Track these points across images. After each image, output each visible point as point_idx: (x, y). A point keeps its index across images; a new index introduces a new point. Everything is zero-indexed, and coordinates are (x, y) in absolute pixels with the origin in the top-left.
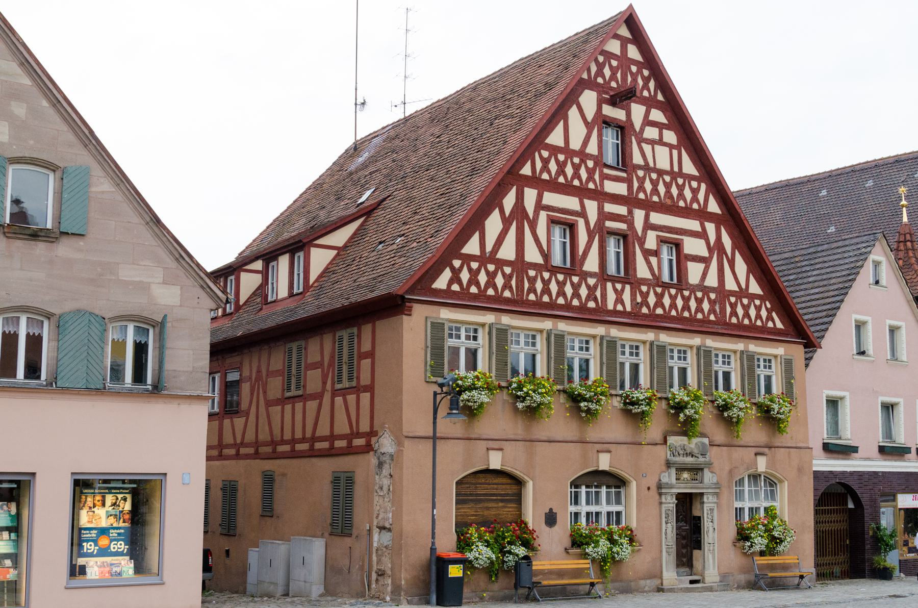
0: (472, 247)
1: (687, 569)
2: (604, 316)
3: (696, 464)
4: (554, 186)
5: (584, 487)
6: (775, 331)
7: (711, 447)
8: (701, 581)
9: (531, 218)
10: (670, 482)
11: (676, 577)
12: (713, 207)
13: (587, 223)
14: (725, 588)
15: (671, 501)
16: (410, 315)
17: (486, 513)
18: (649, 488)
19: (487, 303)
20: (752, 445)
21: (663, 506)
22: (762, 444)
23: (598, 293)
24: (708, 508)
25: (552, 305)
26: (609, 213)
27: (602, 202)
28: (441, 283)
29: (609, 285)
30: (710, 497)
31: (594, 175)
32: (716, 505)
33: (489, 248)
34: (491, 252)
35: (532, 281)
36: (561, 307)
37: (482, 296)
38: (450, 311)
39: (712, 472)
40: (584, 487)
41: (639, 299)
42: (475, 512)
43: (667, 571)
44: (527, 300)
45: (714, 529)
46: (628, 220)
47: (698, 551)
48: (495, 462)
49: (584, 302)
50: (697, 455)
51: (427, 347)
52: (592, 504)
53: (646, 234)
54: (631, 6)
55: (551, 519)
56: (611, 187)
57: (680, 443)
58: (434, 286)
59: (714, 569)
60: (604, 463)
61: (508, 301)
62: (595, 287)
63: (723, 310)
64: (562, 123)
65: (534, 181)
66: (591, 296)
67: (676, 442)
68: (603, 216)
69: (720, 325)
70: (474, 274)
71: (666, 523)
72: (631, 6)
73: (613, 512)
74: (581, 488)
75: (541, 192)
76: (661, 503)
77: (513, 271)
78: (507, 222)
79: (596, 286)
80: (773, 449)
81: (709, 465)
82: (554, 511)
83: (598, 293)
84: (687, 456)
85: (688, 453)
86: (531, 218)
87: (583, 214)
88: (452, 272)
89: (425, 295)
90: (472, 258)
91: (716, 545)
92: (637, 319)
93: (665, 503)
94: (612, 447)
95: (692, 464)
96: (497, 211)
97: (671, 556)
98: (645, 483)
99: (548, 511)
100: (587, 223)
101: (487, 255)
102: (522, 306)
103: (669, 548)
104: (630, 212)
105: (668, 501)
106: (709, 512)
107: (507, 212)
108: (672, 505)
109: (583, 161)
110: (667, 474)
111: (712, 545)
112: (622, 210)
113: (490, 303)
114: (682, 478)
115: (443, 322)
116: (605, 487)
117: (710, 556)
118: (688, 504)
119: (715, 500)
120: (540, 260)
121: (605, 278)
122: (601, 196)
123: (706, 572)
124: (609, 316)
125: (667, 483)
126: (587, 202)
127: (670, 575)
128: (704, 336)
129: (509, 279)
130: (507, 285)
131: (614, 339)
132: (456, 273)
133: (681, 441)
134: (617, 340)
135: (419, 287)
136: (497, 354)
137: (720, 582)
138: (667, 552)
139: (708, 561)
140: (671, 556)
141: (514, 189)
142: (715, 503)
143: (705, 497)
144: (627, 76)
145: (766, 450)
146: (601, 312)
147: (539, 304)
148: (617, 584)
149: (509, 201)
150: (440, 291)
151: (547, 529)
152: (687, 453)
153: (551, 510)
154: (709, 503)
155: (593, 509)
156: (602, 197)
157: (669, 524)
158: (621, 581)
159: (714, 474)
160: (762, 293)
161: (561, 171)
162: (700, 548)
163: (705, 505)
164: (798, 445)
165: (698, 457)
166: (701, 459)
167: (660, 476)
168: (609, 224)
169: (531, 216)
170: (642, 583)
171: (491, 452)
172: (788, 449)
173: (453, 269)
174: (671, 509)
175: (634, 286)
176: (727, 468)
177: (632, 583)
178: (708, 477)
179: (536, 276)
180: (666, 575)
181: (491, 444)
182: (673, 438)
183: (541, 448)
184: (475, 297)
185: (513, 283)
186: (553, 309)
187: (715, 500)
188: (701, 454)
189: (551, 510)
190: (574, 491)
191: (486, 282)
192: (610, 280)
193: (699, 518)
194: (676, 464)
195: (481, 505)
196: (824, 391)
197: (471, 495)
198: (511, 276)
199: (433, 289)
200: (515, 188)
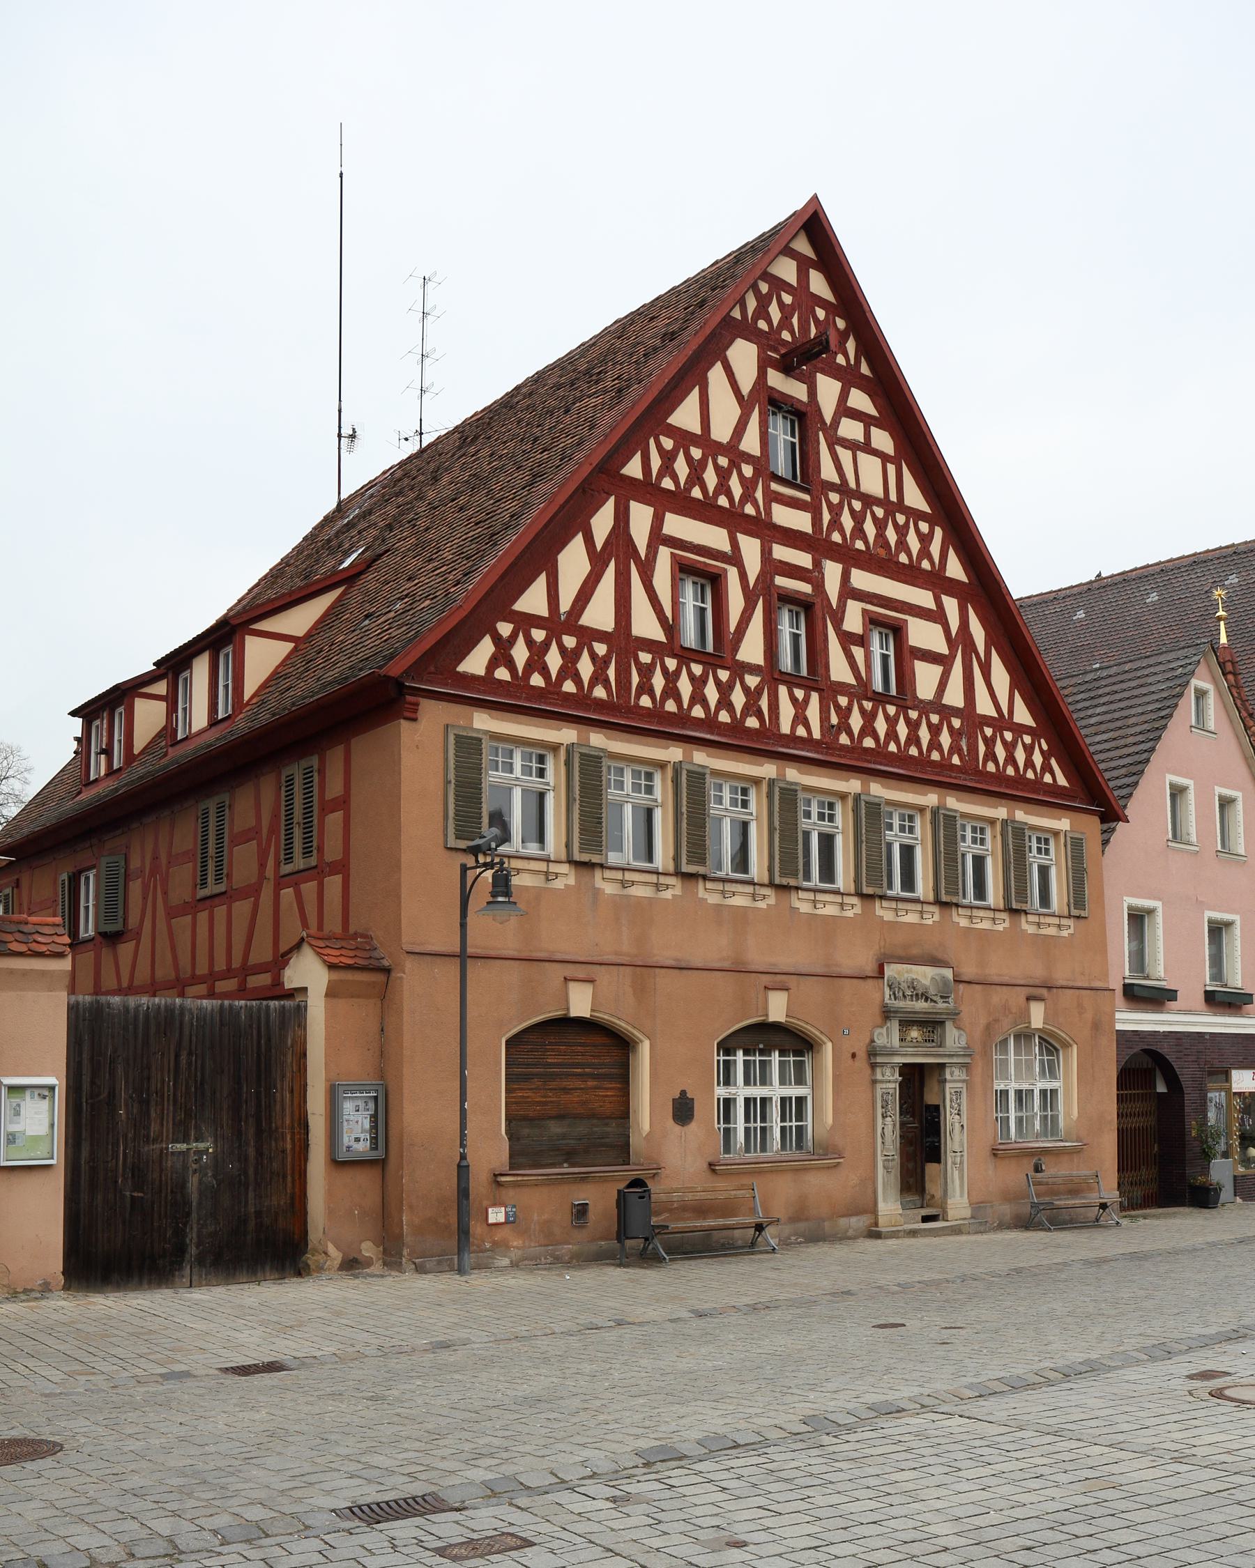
0: (533, 600)
1: (916, 1198)
4: (681, 503)
5: (740, 1053)
6: (1054, 789)
7: (957, 984)
8: (941, 1217)
10: (889, 1045)
11: (901, 1212)
12: (955, 569)
13: (743, 576)
14: (982, 1229)
15: (891, 1078)
16: (415, 720)
18: (854, 1056)
19: (562, 706)
20: (1022, 982)
21: (879, 1086)
22: (1037, 982)
23: (764, 704)
24: (953, 1091)
25: (683, 718)
26: (780, 561)
27: (770, 541)
28: (476, 662)
29: (783, 690)
30: (957, 1072)
31: (754, 491)
33: (565, 605)
34: (569, 613)
35: (646, 671)
36: (698, 723)
37: (553, 693)
38: (492, 717)
39: (958, 1028)
40: (740, 1053)
41: (834, 720)
42: (542, 1097)
43: (885, 1200)
44: (637, 706)
45: (962, 1126)
46: (814, 576)
47: (935, 1165)
48: (580, 1004)
50: (934, 998)
51: (448, 782)
52: (755, 1084)
53: (845, 606)
54: (815, 199)
56: (784, 516)
57: (906, 975)
58: (462, 668)
59: (962, 1195)
60: (777, 1009)
61: (599, 703)
62: (759, 691)
63: (973, 749)
64: (696, 391)
65: (647, 490)
66: (752, 707)
67: (899, 973)
68: (771, 566)
69: (969, 774)
70: (538, 653)
71: (884, 1117)
72: (815, 199)
73: (791, 1098)
74: (735, 1055)
75: (660, 512)
76: (874, 1082)
77: (609, 652)
78: (598, 561)
79: (759, 691)
80: (1055, 990)
81: (954, 1015)
82: (689, 1096)
83: (764, 704)
84: (917, 1000)
85: (920, 993)
87: (735, 558)
91: (965, 1153)
93: (882, 1082)
94: (792, 981)
95: (925, 1013)
96: (579, 540)
99: (677, 1095)
100: (743, 576)
102: (627, 718)
103: (888, 1160)
104: (817, 564)
105: (886, 1078)
106: (954, 1098)
108: (893, 1085)
109: (735, 464)
111: (959, 1154)
112: (803, 559)
113: (569, 708)
114: (909, 1039)
115: (480, 736)
116: (777, 1053)
117: (956, 1173)
118: (917, 1084)
119: (964, 1077)
120: (658, 635)
121: (776, 677)
122: (769, 532)
123: (949, 1201)
124: (783, 746)
125: (885, 1047)
127: (889, 1207)
128: (944, 791)
129: (600, 664)
130: (599, 677)
131: (793, 787)
133: (907, 972)
134: (798, 788)
135: (432, 669)
136: (581, 801)
137: (972, 1217)
138: (884, 1167)
139: (953, 1182)
141: (611, 503)
142: (963, 1081)
143: (948, 1071)
144: (810, 325)
145: (1044, 992)
146: (769, 738)
147: (656, 713)
148: (802, 1226)
149: (602, 522)
150: (474, 678)
151: (677, 1128)
152: (917, 995)
153: (683, 1093)
155: (757, 1092)
156: (769, 533)
157: (889, 1119)
158: (807, 1220)
159: (962, 1032)
161: (696, 476)
162: (939, 1161)
163: (948, 1085)
165: (935, 1002)
166: (941, 1005)
167: (872, 1035)
168: (780, 581)
169: (642, 553)
170: (843, 1222)
171: (572, 985)
172: (1077, 991)
173: (497, 638)
174: (891, 1091)
176: (983, 1021)
177: (826, 1223)
178: (953, 1038)
179: (653, 664)
180: (882, 1206)
181: (570, 971)
182: (894, 966)
183: (665, 982)
185: (611, 673)
187: (964, 1077)
188: (942, 997)
189: (683, 1093)
190: (724, 1060)
191: (561, 667)
192: (785, 682)
193: (937, 1108)
194: (901, 1012)
195: (553, 1085)
196: (1125, 898)
197: (535, 1065)
199: (459, 672)
200: (612, 500)
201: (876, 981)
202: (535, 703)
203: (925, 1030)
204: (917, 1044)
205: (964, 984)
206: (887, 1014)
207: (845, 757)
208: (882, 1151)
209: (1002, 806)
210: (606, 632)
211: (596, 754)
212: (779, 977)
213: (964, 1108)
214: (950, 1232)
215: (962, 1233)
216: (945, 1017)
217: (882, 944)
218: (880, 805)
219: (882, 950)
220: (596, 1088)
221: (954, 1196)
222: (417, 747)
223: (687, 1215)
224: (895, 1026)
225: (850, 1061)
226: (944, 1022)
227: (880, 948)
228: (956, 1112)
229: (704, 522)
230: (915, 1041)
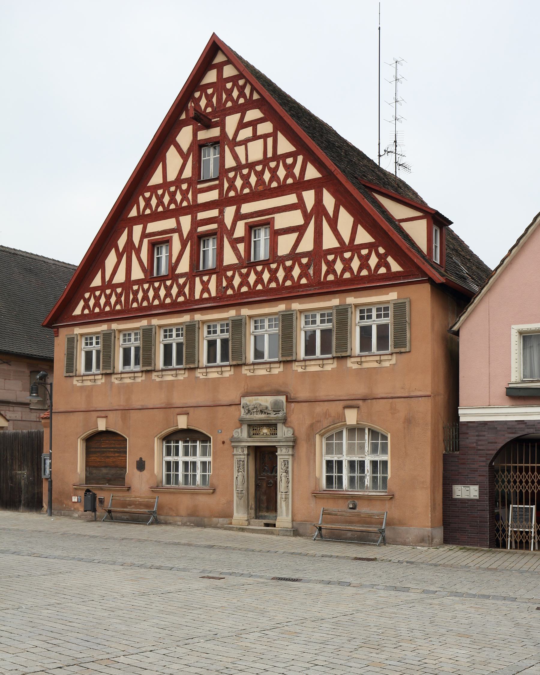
0: (97, 282)
2: (192, 306)
3: (268, 420)
4: (156, 217)
5: (198, 442)
6: (397, 275)
7: (290, 403)
9: (137, 247)
15: (241, 453)
16: (58, 336)
17: (107, 460)
18: (223, 443)
19: (105, 317)
20: (345, 398)
22: (359, 397)
23: (187, 290)
24: (282, 460)
25: (151, 307)
26: (201, 220)
28: (78, 311)
29: (197, 279)
30: (284, 450)
32: (291, 457)
33: (107, 278)
34: (108, 281)
35: (136, 293)
37: (102, 313)
38: (80, 329)
39: (287, 427)
41: (225, 284)
42: (100, 459)
43: (237, 512)
44: (131, 308)
48: (102, 426)
49: (174, 298)
52: (191, 456)
55: (141, 465)
56: (202, 198)
59: (287, 515)
60: (182, 423)
61: (119, 312)
63: (318, 271)
67: (250, 401)
68: (195, 224)
69: (314, 286)
70: (97, 299)
76: (234, 455)
78: (120, 257)
80: (369, 401)
81: (285, 421)
82: (143, 460)
83: (187, 290)
86: (137, 247)
87: (178, 230)
88: (84, 302)
89: (71, 321)
90: (96, 288)
92: (222, 302)
94: (191, 411)
95: (263, 420)
96: (113, 251)
97: (242, 500)
98: (220, 438)
99: (138, 459)
101: (106, 283)
103: (238, 493)
106: (283, 464)
107: (121, 249)
108: (243, 457)
109: (178, 187)
110: (239, 430)
112: (214, 213)
113: (108, 317)
114: (262, 433)
117: (284, 504)
124: (196, 305)
126: (182, 219)
129: (119, 296)
130: (118, 302)
132: (87, 301)
133: (255, 400)
135: (66, 317)
136: (103, 351)
138: (237, 496)
139: (281, 508)
140: (242, 500)
143: (279, 450)
145: (360, 403)
147: (140, 308)
148: (193, 519)
150: (78, 316)
151: (138, 472)
153: (141, 459)
154: (282, 455)
155: (190, 459)
156: (196, 209)
157: (240, 473)
158: (197, 516)
160: (373, 240)
161: (160, 202)
164: (412, 394)
166: (273, 415)
168: (200, 229)
169: (137, 246)
170: (215, 520)
171: (99, 419)
172: (391, 400)
174: (242, 460)
175: (220, 274)
176: (308, 422)
177: (206, 519)
178: (283, 432)
180: (235, 515)
181: (99, 414)
182: (247, 398)
183: (134, 415)
184: (98, 314)
185: (123, 299)
186: (151, 310)
189: (141, 459)
191: (105, 303)
195: (104, 455)
198: (121, 294)
201: (237, 407)
202: (97, 319)
203: (271, 429)
204: (266, 436)
205: (295, 403)
206: (242, 422)
207: (230, 300)
208: (236, 488)
209: (335, 298)
210: (122, 283)
211: (109, 332)
212: (184, 409)
213: (290, 469)
214: (266, 533)
215: (274, 534)
216: (275, 421)
217: (246, 387)
218: (242, 320)
219: (246, 390)
220: (118, 456)
221: (282, 515)
222: (59, 345)
223: (142, 507)
224: (245, 428)
225: (222, 445)
226: (277, 424)
227: (245, 390)
228: (284, 471)
229: (165, 219)
230: (265, 434)
